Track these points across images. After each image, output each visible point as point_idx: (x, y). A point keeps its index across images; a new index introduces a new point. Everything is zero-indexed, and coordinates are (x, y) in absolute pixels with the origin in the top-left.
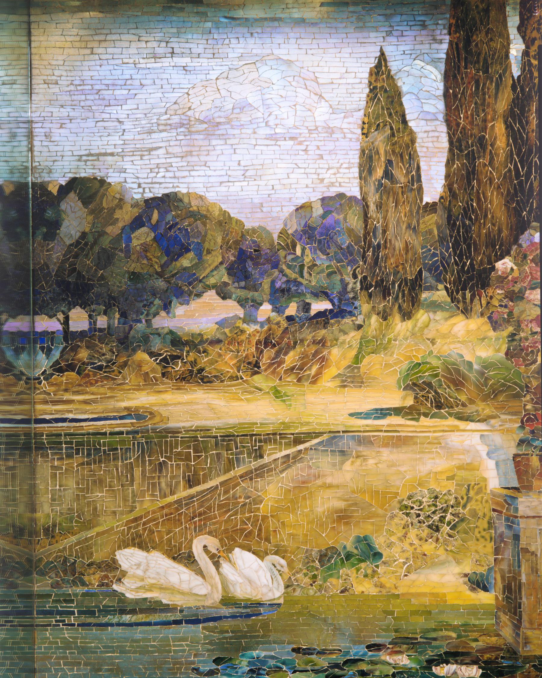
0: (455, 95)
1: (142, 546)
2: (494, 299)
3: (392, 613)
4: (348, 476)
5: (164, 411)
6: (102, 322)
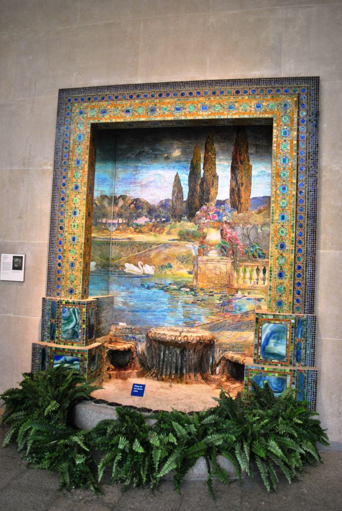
1: (129, 263)
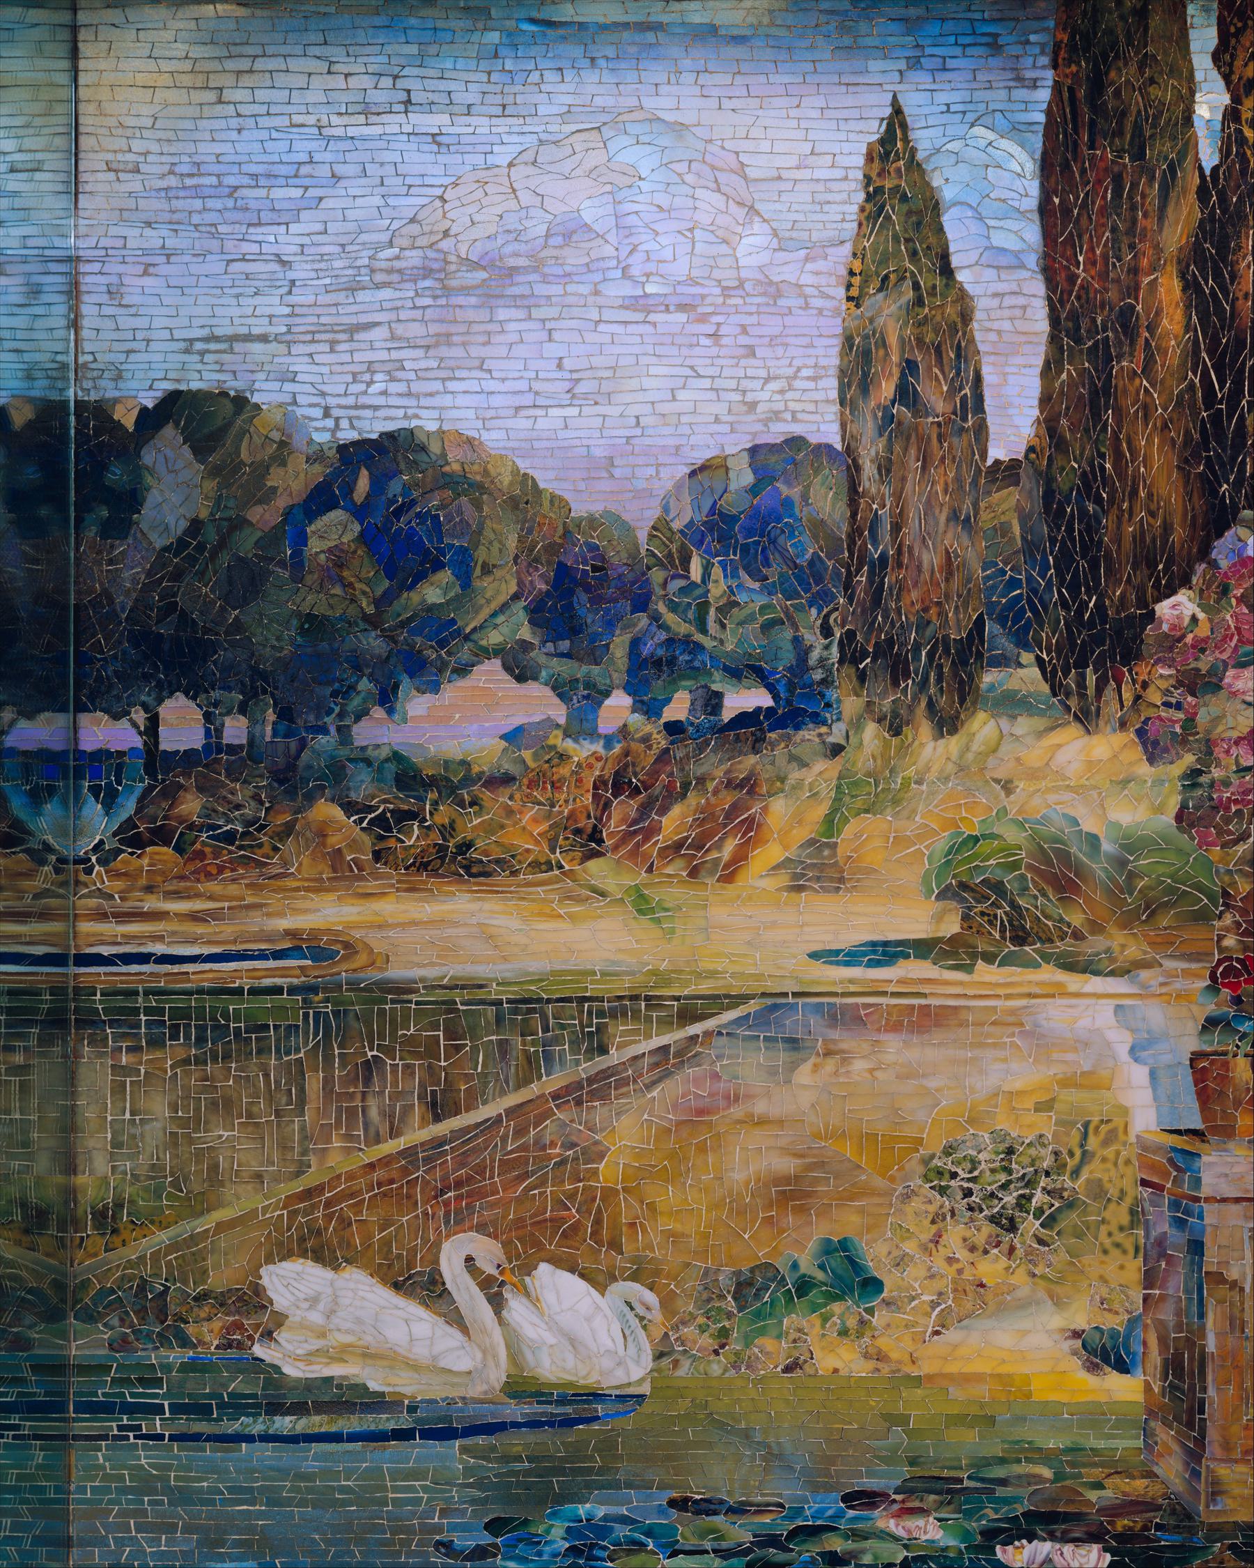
0: (1066, 210)
1: (324, 1255)
2: (1152, 688)
3: (903, 1420)
4: (806, 1099)
5: (377, 942)
6: (235, 729)
